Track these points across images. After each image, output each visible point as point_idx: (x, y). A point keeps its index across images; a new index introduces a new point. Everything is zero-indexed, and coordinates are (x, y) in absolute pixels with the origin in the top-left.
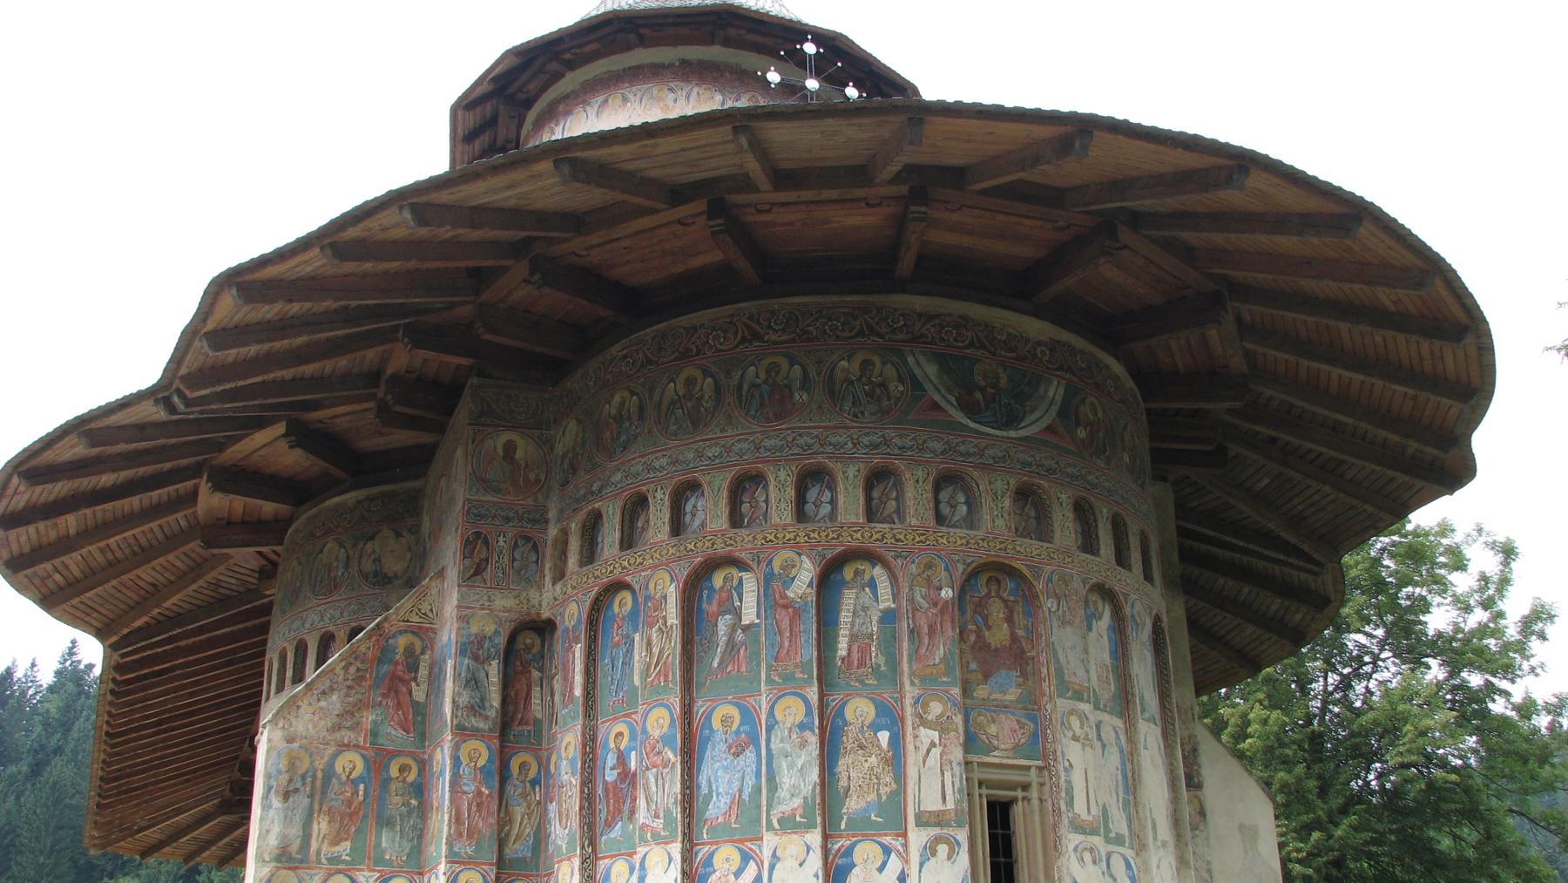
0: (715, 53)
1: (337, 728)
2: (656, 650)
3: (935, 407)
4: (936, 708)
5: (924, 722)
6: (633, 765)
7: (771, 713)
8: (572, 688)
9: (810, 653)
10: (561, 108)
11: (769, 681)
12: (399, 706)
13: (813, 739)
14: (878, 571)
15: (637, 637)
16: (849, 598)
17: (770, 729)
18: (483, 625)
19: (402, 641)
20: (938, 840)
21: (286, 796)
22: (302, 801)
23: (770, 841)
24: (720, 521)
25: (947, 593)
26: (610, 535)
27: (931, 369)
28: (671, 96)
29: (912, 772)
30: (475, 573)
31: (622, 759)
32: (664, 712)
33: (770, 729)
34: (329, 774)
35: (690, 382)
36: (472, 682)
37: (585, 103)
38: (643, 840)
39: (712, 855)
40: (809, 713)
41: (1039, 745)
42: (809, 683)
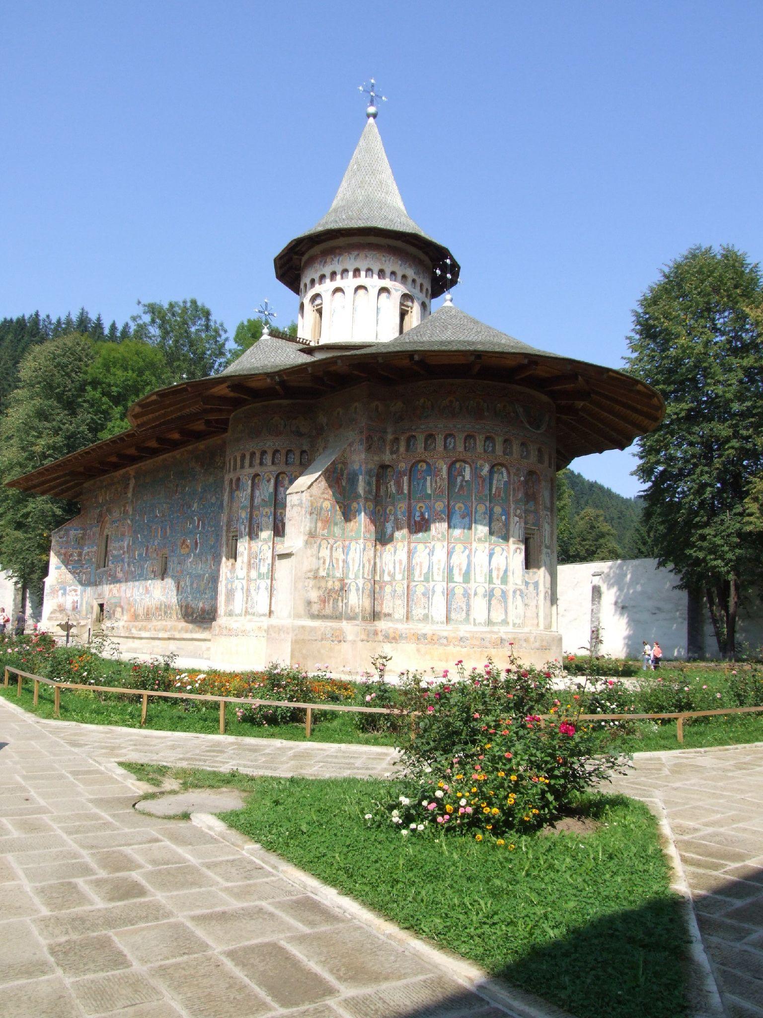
0: (399, 244)
1: (323, 493)
2: (439, 484)
3: (522, 422)
4: (518, 511)
5: (516, 516)
6: (426, 517)
7: (476, 509)
8: (403, 488)
9: (487, 492)
10: (337, 251)
11: (475, 499)
12: (339, 487)
13: (487, 517)
14: (504, 470)
15: (429, 478)
16: (496, 476)
17: (475, 513)
18: (371, 466)
19: (340, 466)
20: (517, 548)
21: (311, 514)
22: (314, 516)
23: (474, 545)
24: (460, 448)
25: (522, 479)
26: (420, 445)
27: (521, 410)
28: (384, 259)
29: (511, 528)
30: (369, 449)
31: (422, 515)
32: (441, 503)
33: (475, 513)
34: (321, 508)
35: (451, 402)
36: (369, 484)
37: (349, 253)
38: (433, 539)
39: (454, 546)
40: (486, 509)
41: (537, 523)
42: (486, 500)
